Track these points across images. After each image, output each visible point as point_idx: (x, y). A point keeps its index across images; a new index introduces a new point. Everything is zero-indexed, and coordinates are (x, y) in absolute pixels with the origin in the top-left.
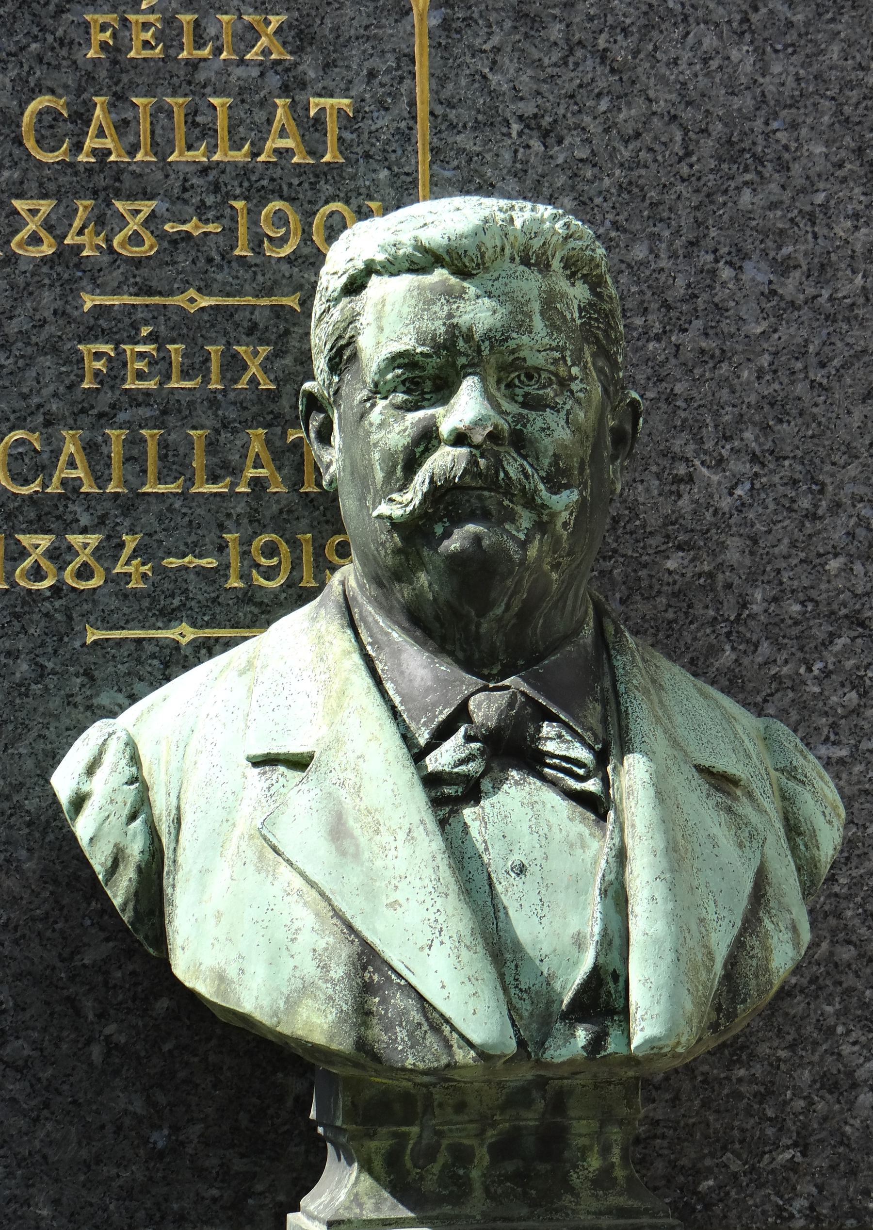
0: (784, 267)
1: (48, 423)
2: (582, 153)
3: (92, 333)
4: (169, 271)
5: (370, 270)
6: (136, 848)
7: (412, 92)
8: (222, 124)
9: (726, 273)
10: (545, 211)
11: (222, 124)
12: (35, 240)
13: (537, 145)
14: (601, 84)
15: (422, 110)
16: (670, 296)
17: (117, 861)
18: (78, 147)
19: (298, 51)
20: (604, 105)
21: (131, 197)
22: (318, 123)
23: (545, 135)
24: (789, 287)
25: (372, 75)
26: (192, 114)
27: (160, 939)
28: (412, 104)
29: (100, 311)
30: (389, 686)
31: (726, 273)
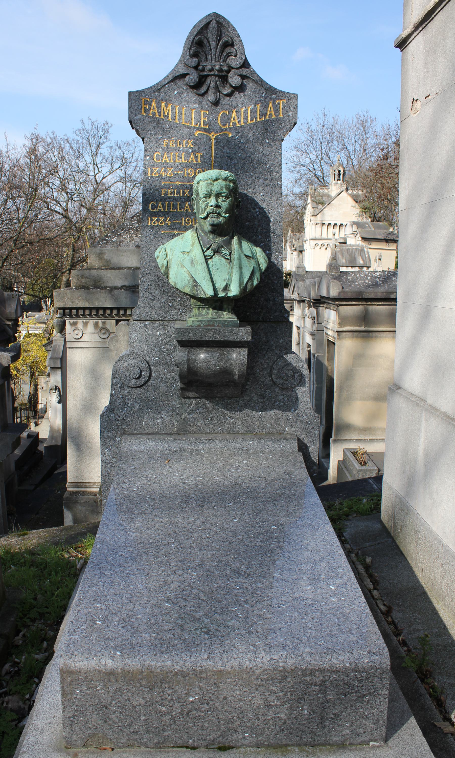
0: (266, 180)
1: (157, 201)
2: (236, 162)
3: (163, 188)
4: (175, 179)
5: (200, 180)
6: (165, 264)
7: (211, 152)
8: (183, 157)
9: (257, 180)
10: (227, 172)
11: (183, 157)
12: (155, 174)
13: (229, 161)
14: (239, 151)
15: (213, 155)
16: (248, 184)
17: (163, 265)
18: (162, 160)
19: (195, 146)
20: (240, 155)
21: (169, 168)
22: (197, 157)
23: (231, 159)
24: (266, 183)
25: (205, 149)
26: (179, 155)
27: (168, 277)
28: (211, 154)
29: (165, 185)
30: (201, 242)
31: (257, 180)
